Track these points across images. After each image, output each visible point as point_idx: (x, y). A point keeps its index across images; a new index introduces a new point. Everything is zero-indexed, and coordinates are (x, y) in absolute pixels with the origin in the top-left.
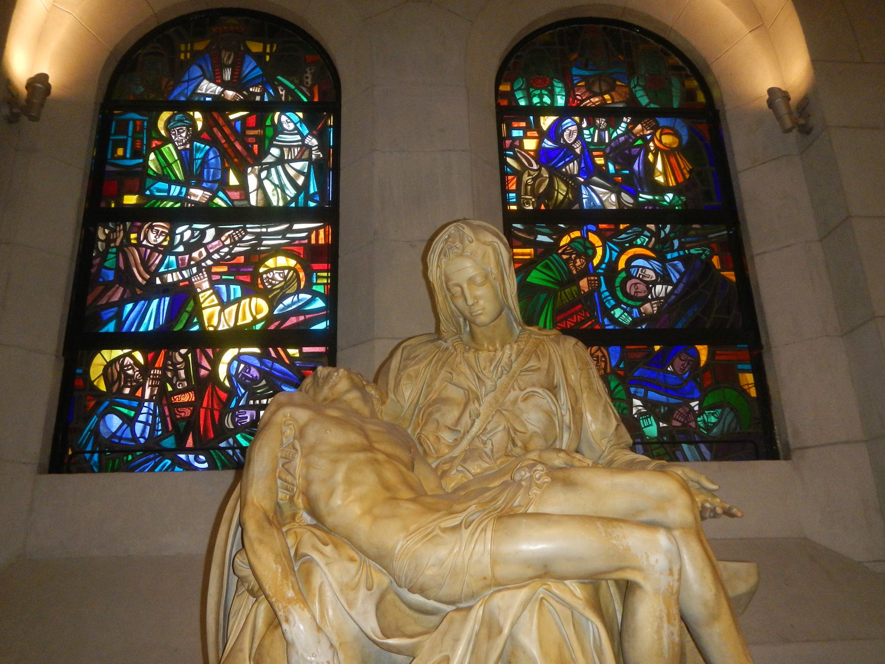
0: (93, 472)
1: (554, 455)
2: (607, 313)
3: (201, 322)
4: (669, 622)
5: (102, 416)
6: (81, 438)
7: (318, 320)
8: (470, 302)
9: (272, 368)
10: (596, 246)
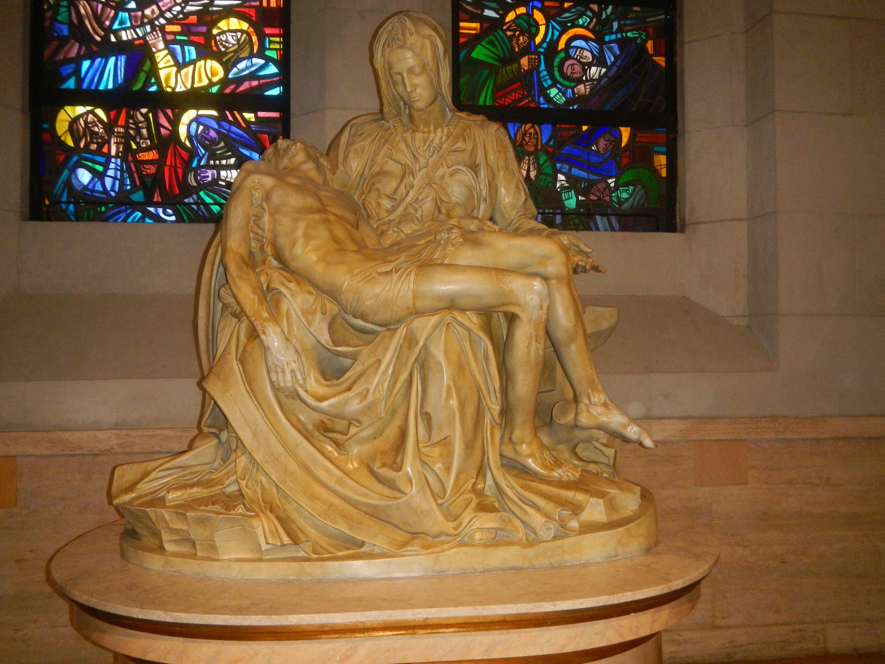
0: (71, 220)
1: (469, 221)
2: (543, 92)
3: (158, 82)
4: (536, 340)
5: (73, 170)
6: (56, 190)
7: (272, 86)
8: (409, 90)
9: (229, 131)
10: (540, 24)
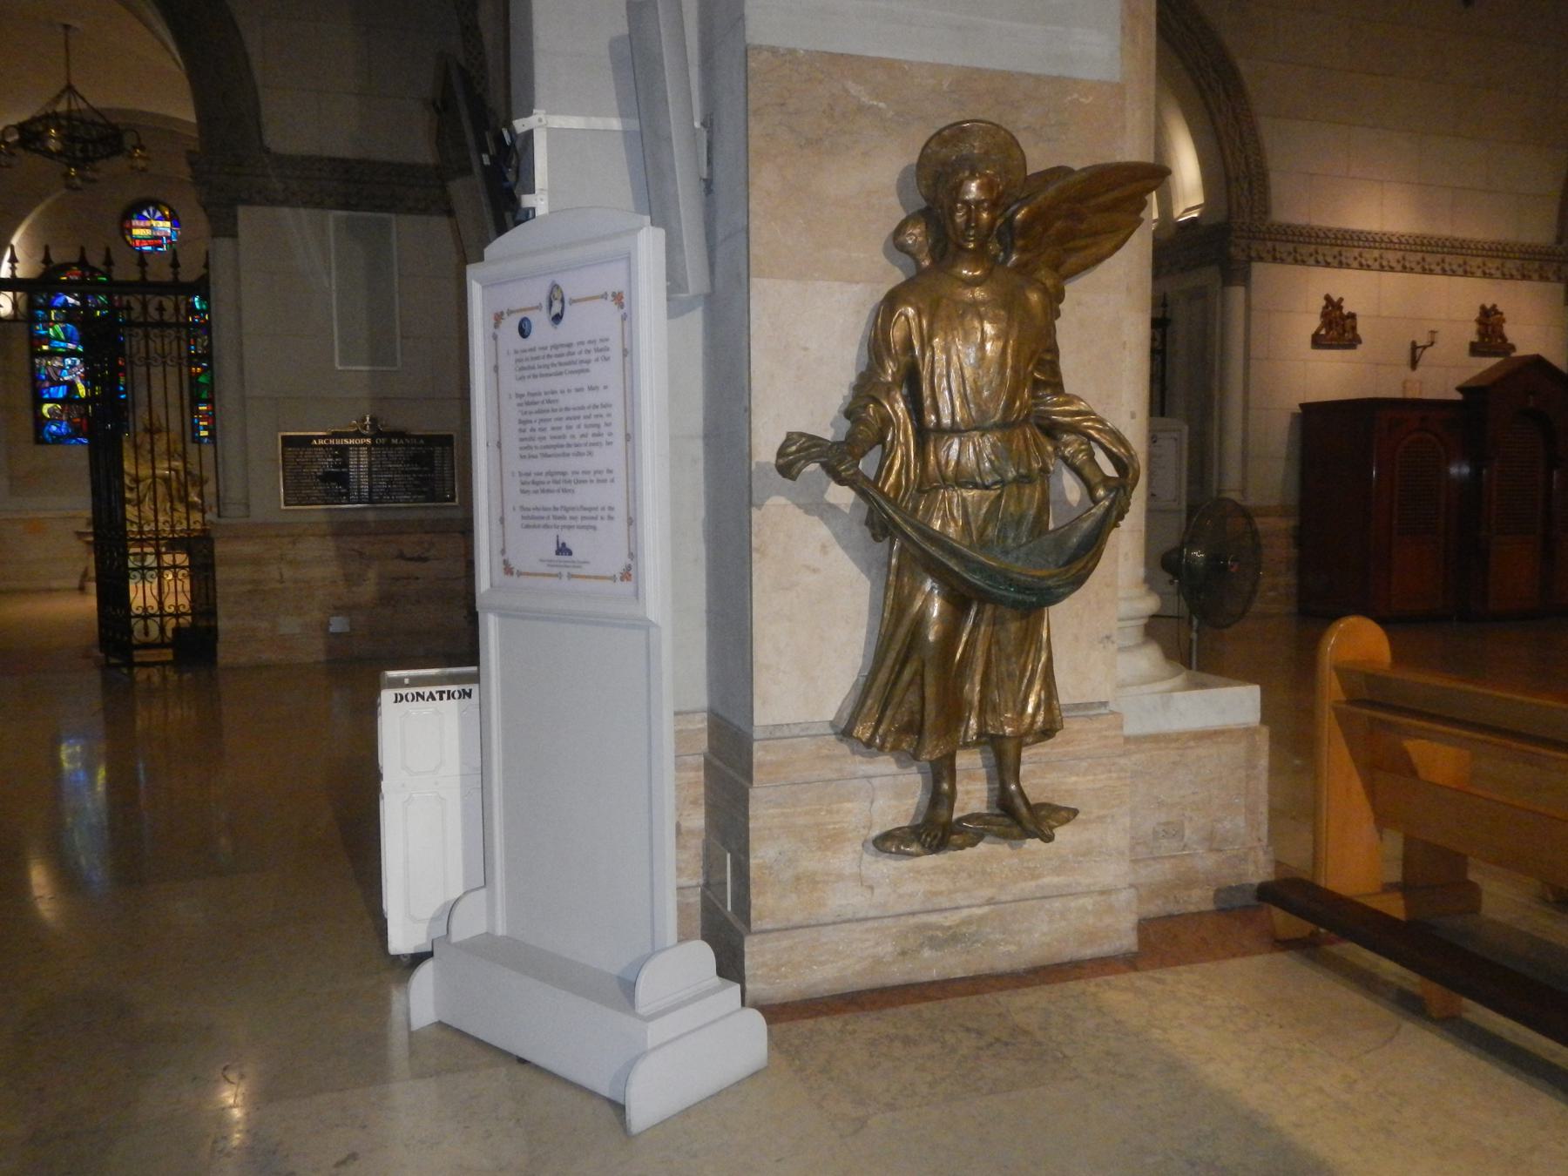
5: (50, 427)
